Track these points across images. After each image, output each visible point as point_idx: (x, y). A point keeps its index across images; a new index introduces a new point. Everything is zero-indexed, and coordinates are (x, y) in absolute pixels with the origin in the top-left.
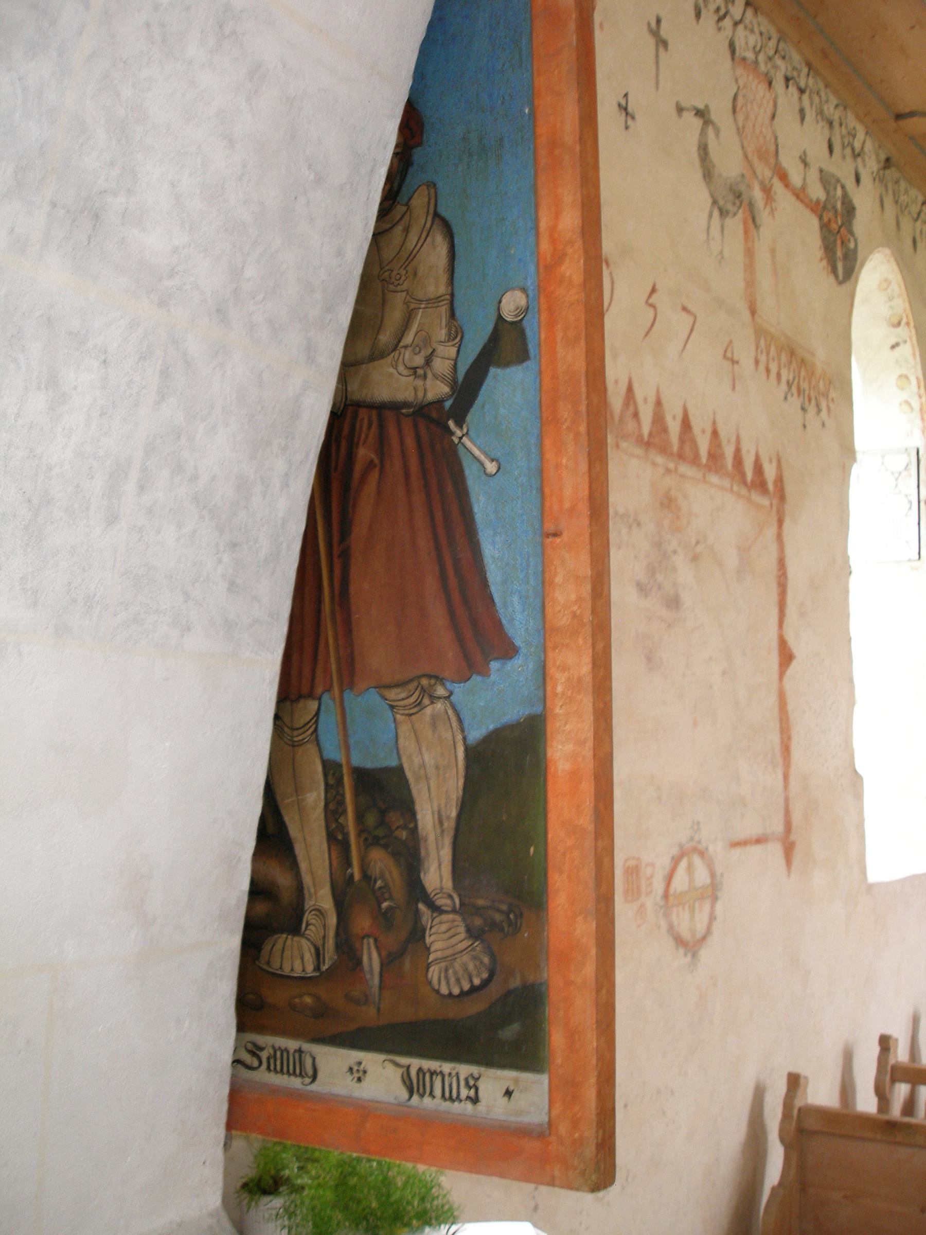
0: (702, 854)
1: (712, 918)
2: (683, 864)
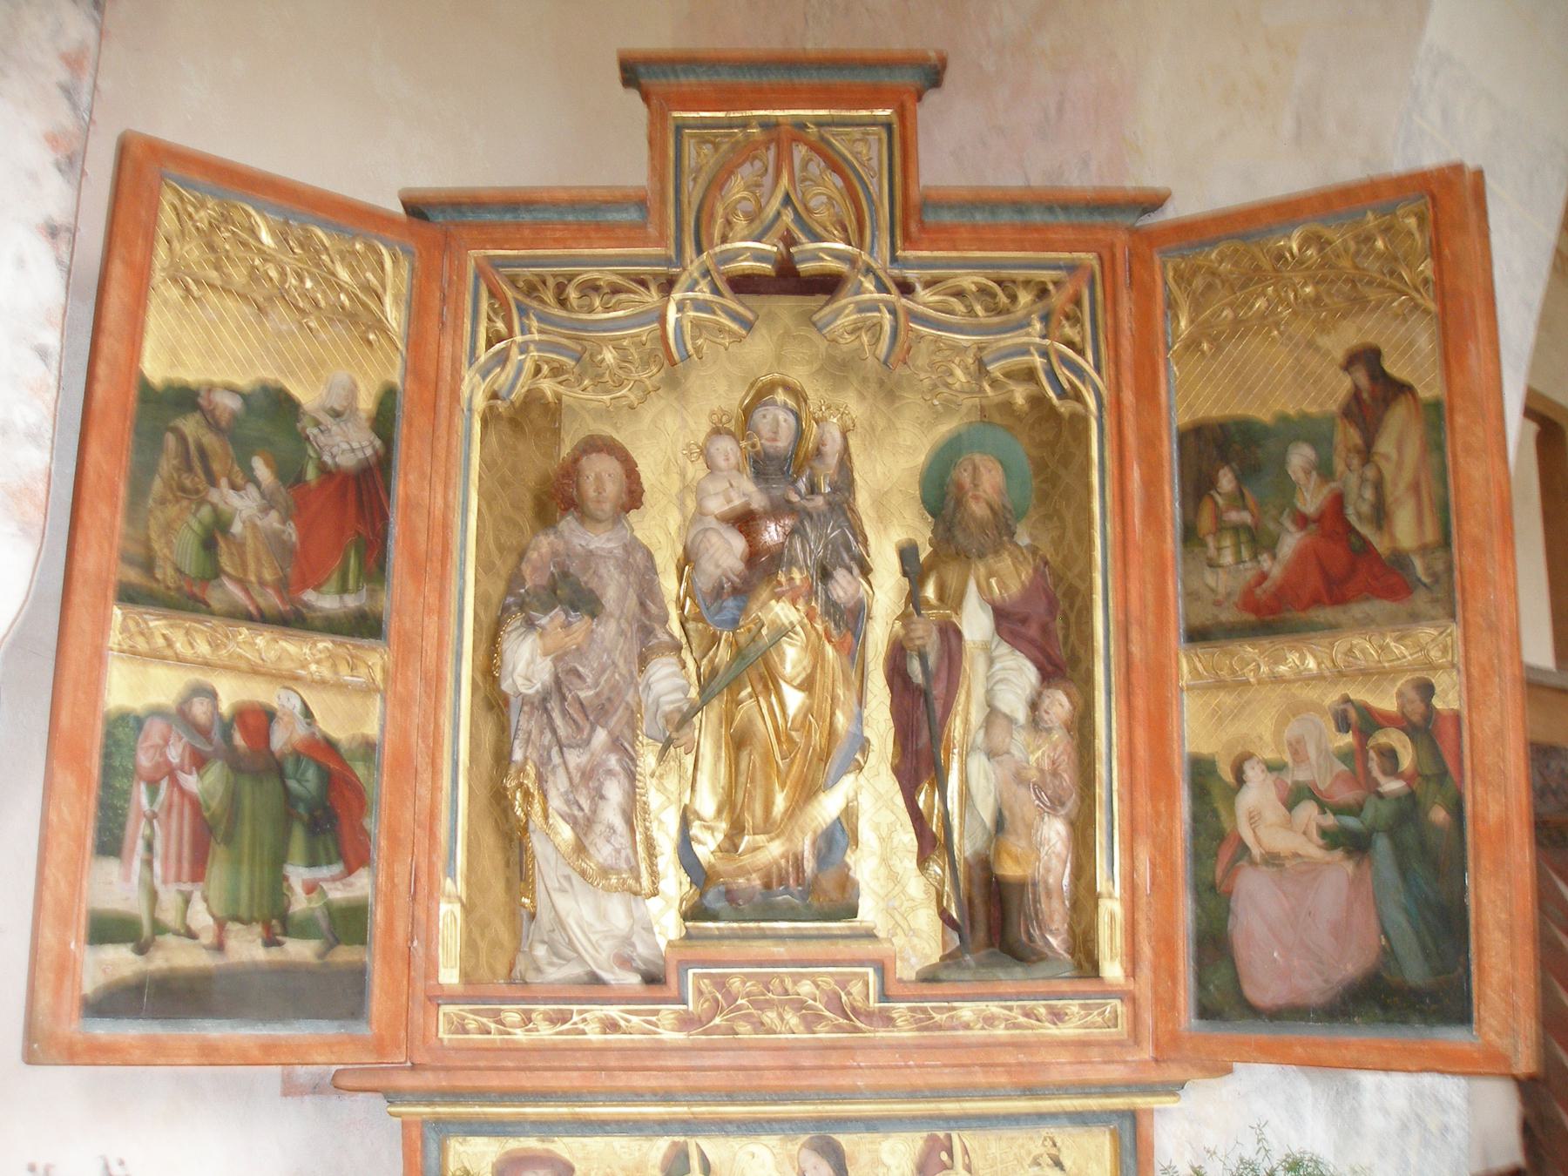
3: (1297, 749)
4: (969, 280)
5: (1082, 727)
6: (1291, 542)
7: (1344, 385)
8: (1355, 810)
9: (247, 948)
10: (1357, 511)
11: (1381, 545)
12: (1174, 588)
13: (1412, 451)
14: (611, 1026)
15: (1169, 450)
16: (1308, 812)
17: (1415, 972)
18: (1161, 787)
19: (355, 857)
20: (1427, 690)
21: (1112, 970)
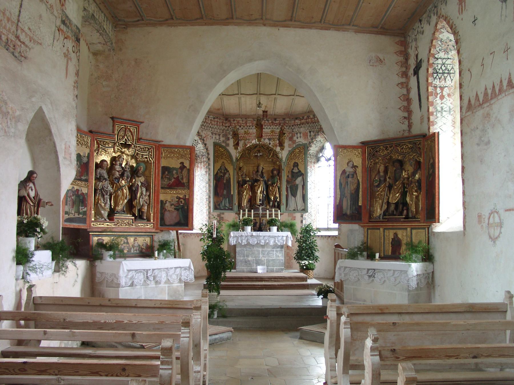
0: (497, 213)
1: (501, 233)
2: (492, 215)
3: (172, 200)
4: (142, 146)
5: (149, 196)
6: (173, 180)
7: (180, 165)
8: (178, 206)
9: (77, 216)
10: (180, 178)
11: (182, 182)
12: (160, 183)
13: (186, 173)
14: (108, 225)
15: (160, 168)
16: (173, 206)
17: (183, 222)
18: (158, 203)
19: (85, 206)
20: (185, 196)
21: (152, 221)
